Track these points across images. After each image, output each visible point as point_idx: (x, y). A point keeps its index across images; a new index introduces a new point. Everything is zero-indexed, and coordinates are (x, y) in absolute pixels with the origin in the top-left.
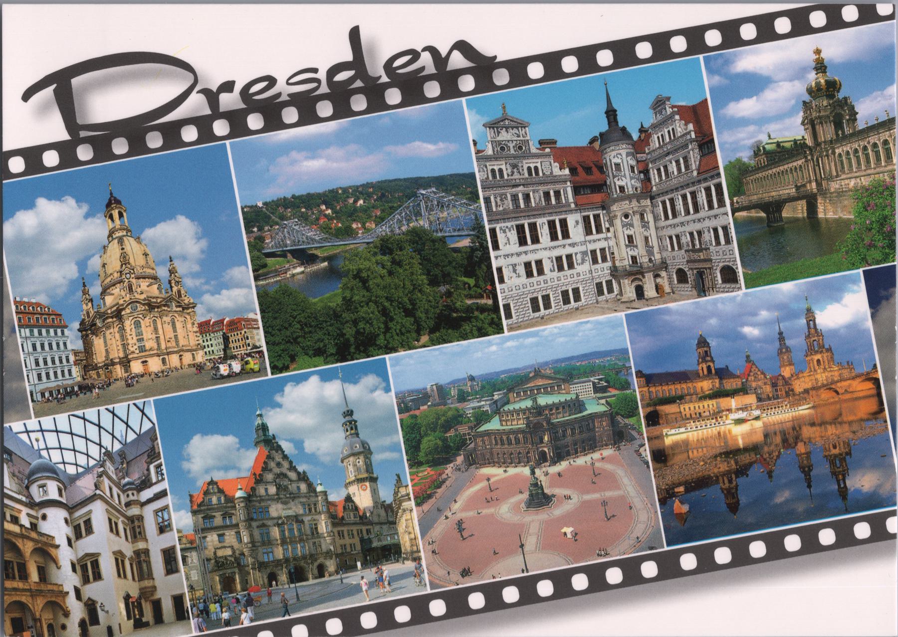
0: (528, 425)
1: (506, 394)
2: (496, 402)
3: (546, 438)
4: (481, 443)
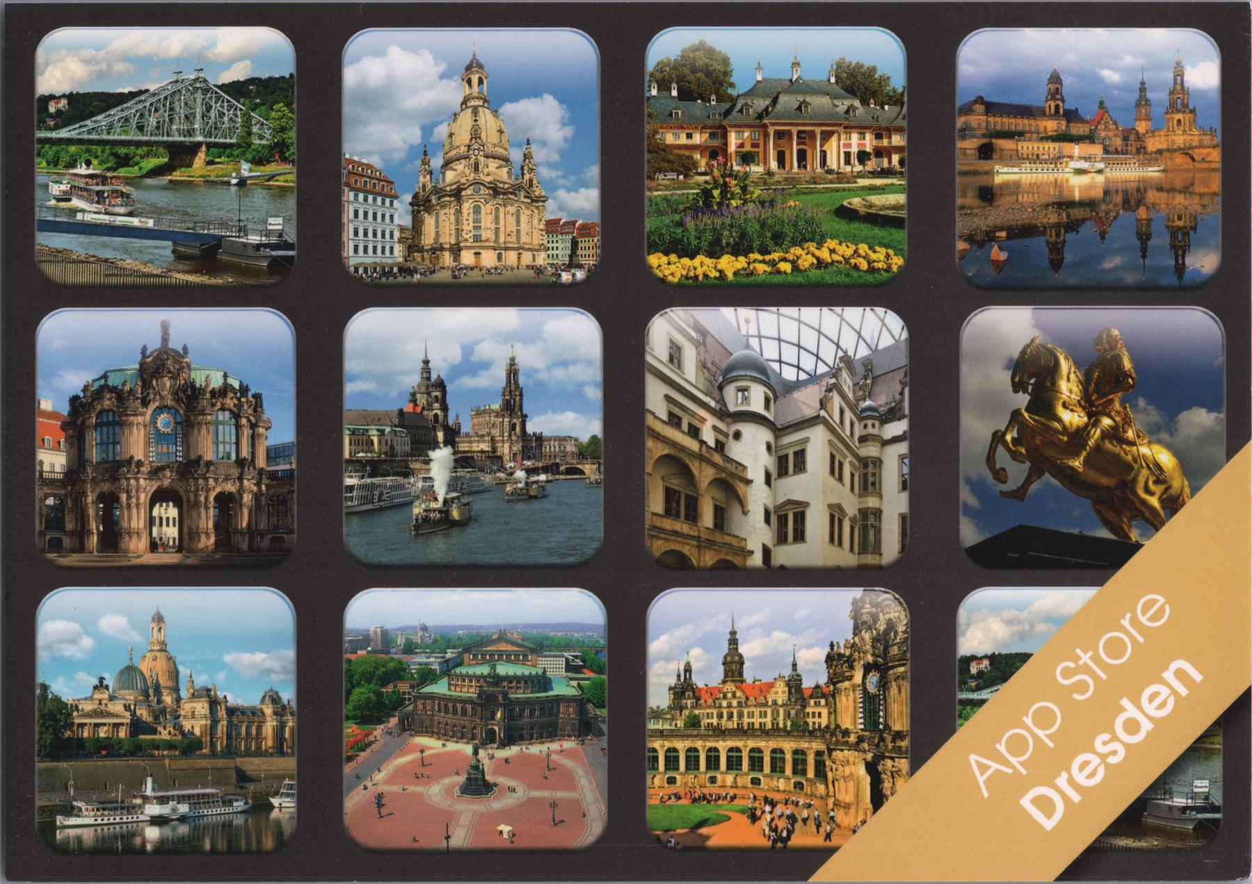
0: (480, 695)
1: (460, 654)
2: (447, 661)
3: (499, 715)
4: (420, 707)
